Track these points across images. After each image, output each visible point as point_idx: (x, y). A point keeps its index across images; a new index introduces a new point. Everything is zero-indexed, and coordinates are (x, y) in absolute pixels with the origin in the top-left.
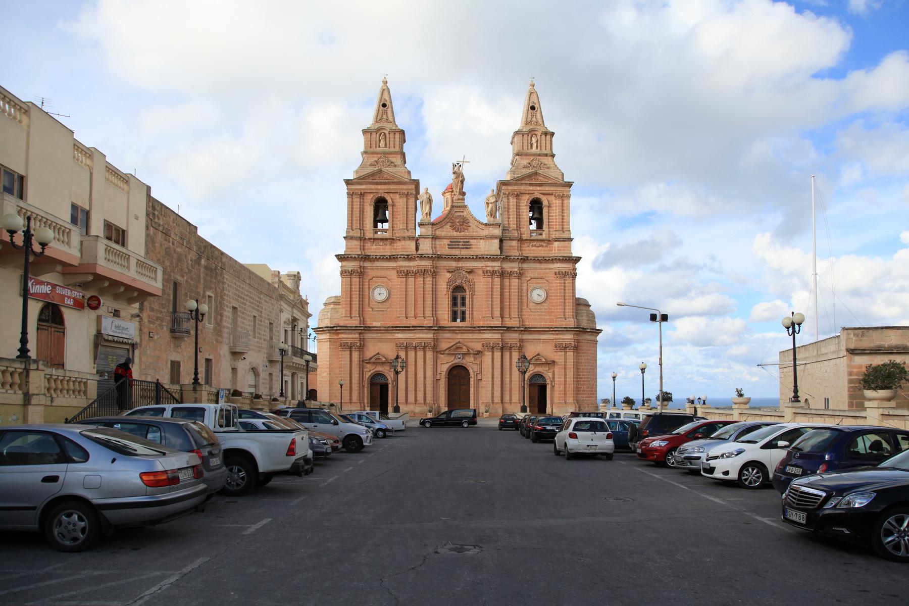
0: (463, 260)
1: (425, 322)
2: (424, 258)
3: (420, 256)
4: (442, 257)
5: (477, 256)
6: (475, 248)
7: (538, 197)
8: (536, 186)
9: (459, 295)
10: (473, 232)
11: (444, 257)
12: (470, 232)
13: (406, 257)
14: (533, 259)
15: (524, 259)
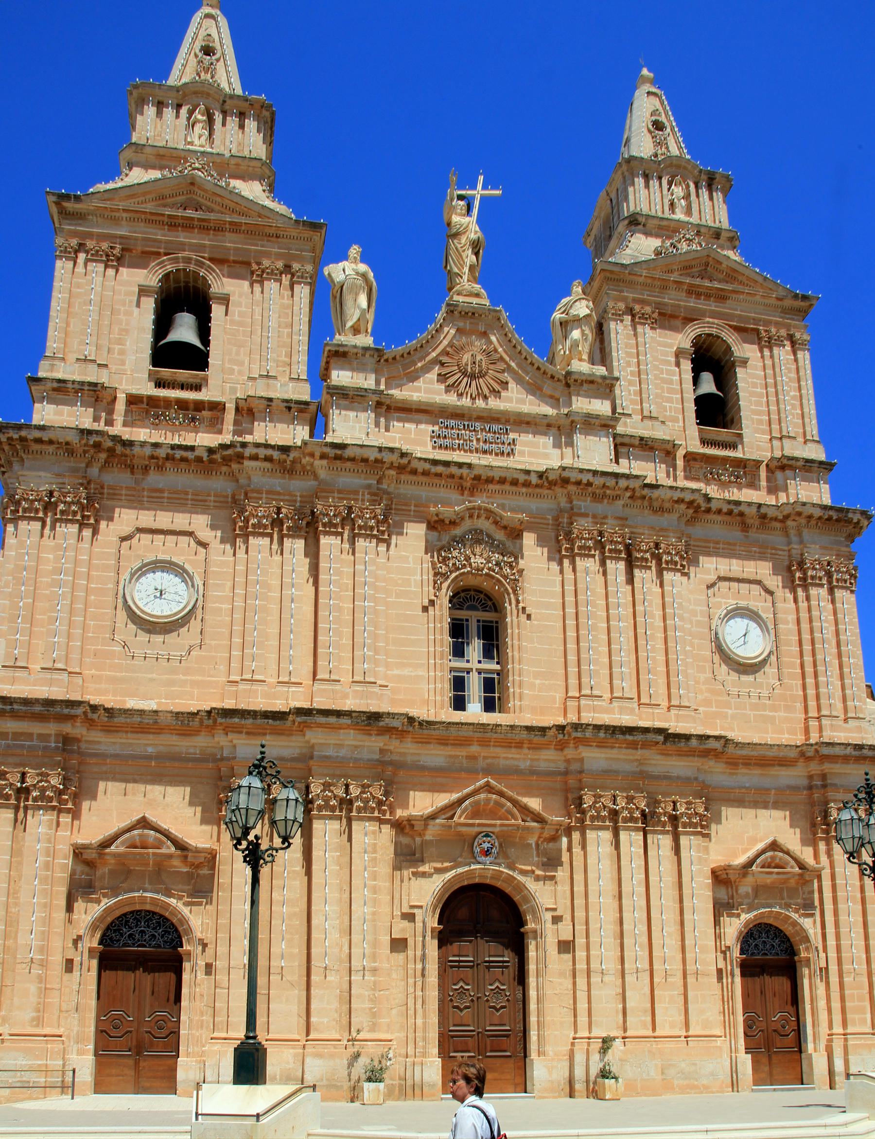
0: (491, 487)
1: (348, 702)
2: (349, 464)
3: (332, 452)
4: (414, 472)
5: (541, 475)
6: (531, 454)
7: (714, 331)
8: (708, 296)
9: (474, 618)
10: (523, 402)
11: (421, 466)
12: (510, 400)
13: (276, 455)
14: (725, 510)
15: (697, 509)
